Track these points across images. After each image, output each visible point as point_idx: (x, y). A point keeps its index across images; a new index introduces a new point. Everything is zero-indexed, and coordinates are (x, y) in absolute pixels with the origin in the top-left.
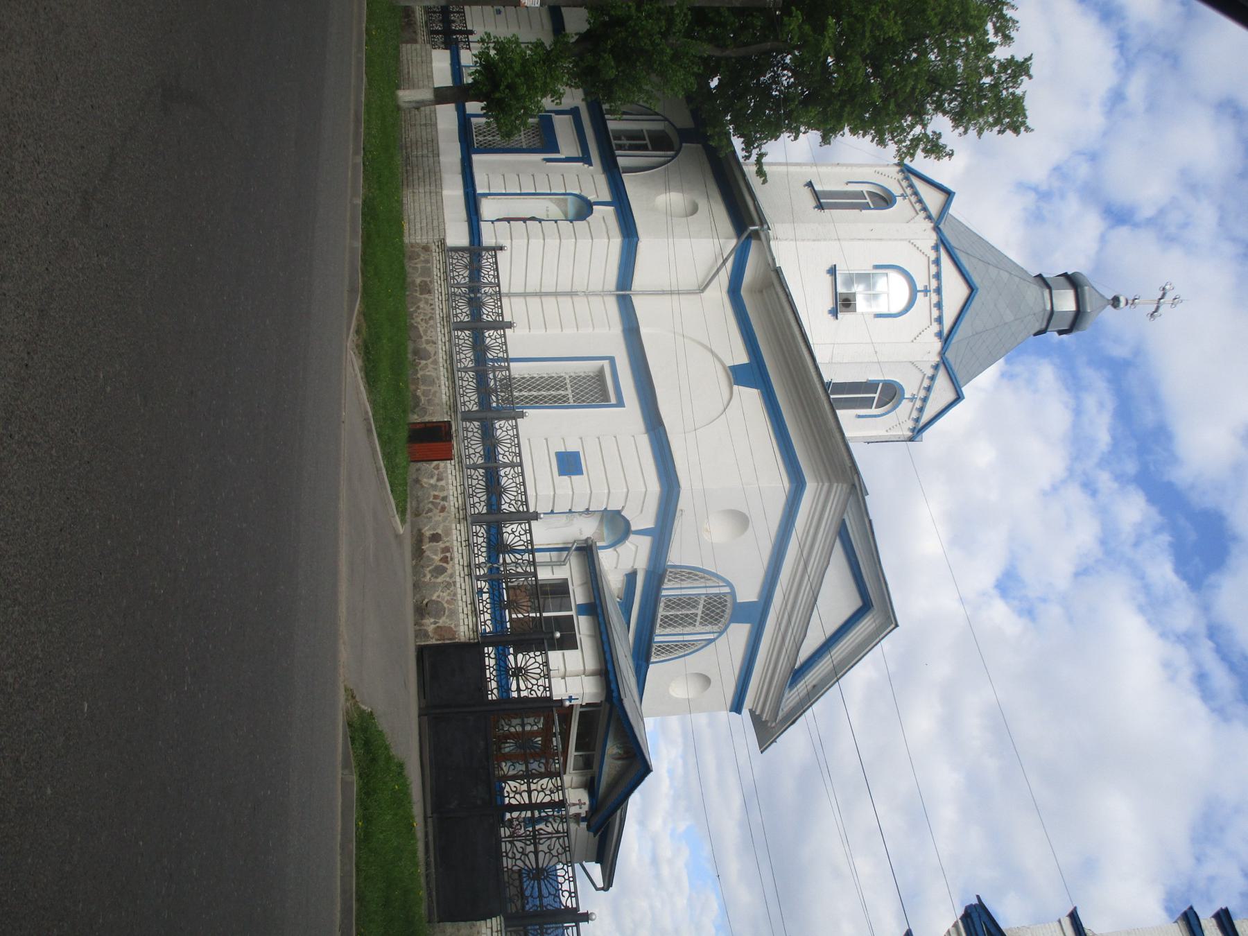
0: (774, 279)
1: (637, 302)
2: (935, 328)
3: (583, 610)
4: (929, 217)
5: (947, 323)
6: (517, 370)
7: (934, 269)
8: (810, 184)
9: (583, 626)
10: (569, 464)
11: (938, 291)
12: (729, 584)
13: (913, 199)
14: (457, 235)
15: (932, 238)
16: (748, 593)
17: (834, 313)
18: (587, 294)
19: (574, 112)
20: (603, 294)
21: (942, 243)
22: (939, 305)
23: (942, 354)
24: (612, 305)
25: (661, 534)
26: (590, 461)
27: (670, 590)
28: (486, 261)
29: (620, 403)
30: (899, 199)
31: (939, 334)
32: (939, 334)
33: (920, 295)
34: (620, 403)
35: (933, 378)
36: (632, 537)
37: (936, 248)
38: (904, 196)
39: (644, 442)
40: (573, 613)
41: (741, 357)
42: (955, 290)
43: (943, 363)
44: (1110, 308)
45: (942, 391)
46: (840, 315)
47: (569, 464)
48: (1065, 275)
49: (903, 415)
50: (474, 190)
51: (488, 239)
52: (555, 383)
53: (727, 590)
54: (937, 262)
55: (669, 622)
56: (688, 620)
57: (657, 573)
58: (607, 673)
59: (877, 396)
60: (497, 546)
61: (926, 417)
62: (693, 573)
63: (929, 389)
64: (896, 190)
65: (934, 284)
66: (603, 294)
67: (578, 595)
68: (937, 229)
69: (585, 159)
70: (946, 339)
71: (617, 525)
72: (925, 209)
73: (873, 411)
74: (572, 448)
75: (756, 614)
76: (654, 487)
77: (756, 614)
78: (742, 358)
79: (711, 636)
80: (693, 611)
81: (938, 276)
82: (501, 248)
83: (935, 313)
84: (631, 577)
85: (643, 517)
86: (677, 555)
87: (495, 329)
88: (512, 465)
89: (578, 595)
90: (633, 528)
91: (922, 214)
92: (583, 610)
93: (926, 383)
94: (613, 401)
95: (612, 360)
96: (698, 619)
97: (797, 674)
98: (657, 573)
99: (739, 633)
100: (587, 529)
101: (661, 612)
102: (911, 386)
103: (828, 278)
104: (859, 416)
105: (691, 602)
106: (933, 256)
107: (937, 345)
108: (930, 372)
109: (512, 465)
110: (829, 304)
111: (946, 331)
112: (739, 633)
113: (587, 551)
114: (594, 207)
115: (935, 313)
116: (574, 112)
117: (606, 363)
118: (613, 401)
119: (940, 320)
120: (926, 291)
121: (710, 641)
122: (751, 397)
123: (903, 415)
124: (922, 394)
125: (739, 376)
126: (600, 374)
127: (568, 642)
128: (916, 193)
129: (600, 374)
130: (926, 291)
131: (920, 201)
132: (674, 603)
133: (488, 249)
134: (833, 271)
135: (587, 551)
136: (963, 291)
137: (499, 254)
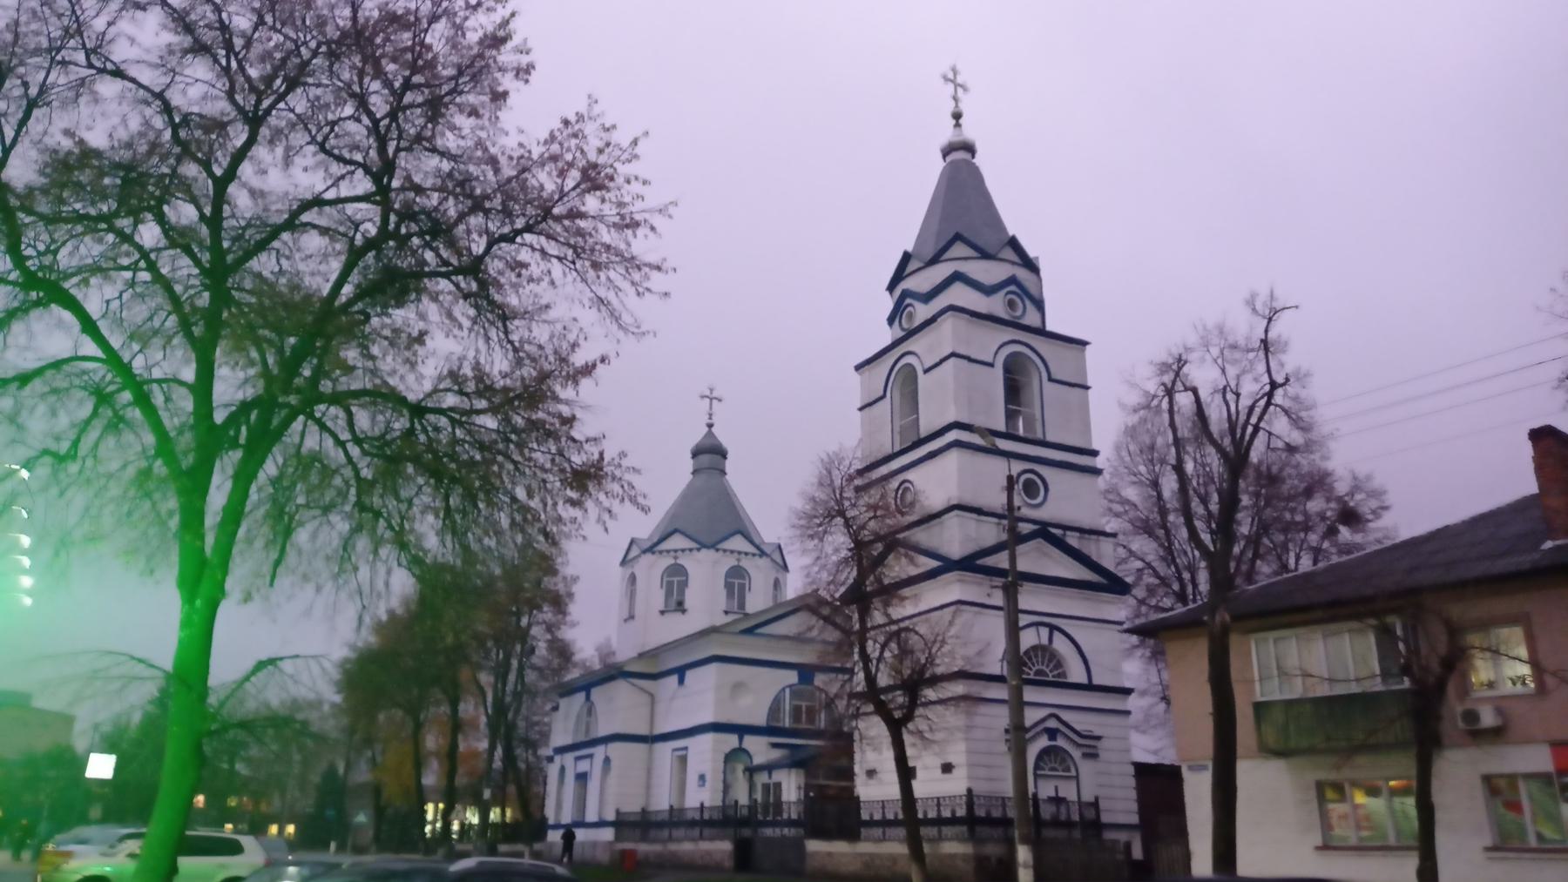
2: (695, 552)
5: (693, 545)
11: (676, 551)
12: (784, 689)
14: (608, 834)
15: (649, 556)
16: (792, 677)
20: (651, 752)
21: (651, 550)
22: (683, 550)
25: (742, 730)
27: (787, 723)
29: (686, 748)
32: (698, 550)
33: (678, 562)
35: (725, 551)
37: (653, 553)
41: (674, 679)
42: (677, 542)
44: (713, 429)
49: (752, 565)
53: (788, 691)
54: (661, 552)
59: (736, 581)
63: (732, 552)
64: (629, 571)
65: (672, 554)
69: (591, 756)
70: (703, 545)
78: (674, 679)
80: (804, 709)
81: (668, 551)
83: (688, 552)
84: (775, 746)
85: (732, 741)
86: (760, 719)
93: (728, 553)
95: (675, 750)
101: (804, 726)
102: (731, 561)
105: (796, 712)
107: (704, 551)
108: (721, 553)
110: (678, 615)
111: (698, 546)
113: (751, 771)
115: (688, 552)
116: (578, 759)
119: (691, 550)
120: (676, 558)
122: (690, 675)
123: (752, 565)
124: (736, 555)
125: (681, 681)
127: (778, 786)
130: (676, 558)
134: (662, 613)
135: (751, 771)
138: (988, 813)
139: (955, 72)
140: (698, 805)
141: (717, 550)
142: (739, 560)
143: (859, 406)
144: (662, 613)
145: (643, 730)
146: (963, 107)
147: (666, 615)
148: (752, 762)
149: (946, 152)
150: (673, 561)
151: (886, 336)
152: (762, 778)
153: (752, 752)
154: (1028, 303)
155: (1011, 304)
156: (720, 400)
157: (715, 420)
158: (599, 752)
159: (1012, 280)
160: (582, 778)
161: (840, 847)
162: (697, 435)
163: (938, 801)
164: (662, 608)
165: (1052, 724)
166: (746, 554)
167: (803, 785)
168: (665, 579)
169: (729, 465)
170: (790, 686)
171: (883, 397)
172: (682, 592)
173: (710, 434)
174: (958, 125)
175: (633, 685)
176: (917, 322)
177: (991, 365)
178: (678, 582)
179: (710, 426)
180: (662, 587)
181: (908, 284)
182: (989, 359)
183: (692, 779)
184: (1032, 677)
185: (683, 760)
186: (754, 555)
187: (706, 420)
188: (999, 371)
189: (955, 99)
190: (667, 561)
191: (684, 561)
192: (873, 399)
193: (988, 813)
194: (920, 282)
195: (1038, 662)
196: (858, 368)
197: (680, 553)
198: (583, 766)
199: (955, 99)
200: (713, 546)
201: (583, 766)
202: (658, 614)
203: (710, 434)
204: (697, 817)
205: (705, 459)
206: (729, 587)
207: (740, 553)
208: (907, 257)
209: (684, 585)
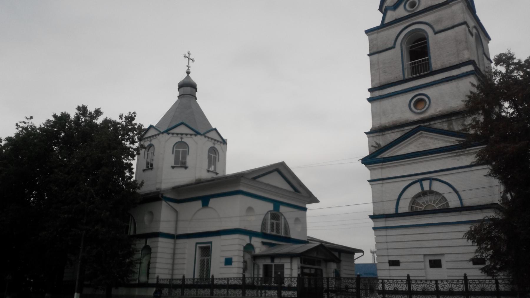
0: (177, 189)
1: (180, 232)
2: (193, 136)
3: (273, 261)
4: (158, 134)
5: (192, 132)
6: (197, 276)
7: (175, 135)
9: (277, 261)
11: (182, 134)
12: (267, 213)
13: (152, 138)
15: (165, 135)
16: (270, 207)
17: (186, 168)
18: (174, 249)
20: (175, 244)
21: (167, 132)
22: (187, 134)
24: (179, 241)
25: (251, 234)
26: (228, 255)
28: (161, 282)
29: (211, 243)
30: (152, 143)
32: (196, 135)
33: (183, 140)
34: (211, 243)
35: (209, 138)
36: (252, 243)
37: (168, 134)
38: (151, 141)
39: (224, 237)
40: (273, 264)
41: (199, 203)
42: (182, 129)
43: (204, 135)
44: (190, 75)
45: (212, 135)
46: (187, 166)
47: (228, 262)
48: (179, 89)
51: (155, 281)
52: (202, 263)
53: (269, 213)
54: (173, 134)
55: (278, 230)
56: (278, 225)
57: (263, 235)
58: (291, 256)
60: (252, 287)
61: (220, 139)
62: (264, 224)
63: (212, 139)
66: (175, 244)
67: (268, 262)
68: (163, 133)
70: (197, 133)
71: (249, 248)
72: (155, 135)
73: (217, 156)
74: (223, 260)
75: (277, 204)
76: (236, 236)
77: (277, 204)
78: (199, 203)
79: (283, 218)
81: (177, 134)
82: (158, 277)
83: (189, 136)
84: (264, 243)
85: (246, 239)
87: (185, 281)
88: (228, 281)
89: (268, 262)
91: (157, 136)
92: (273, 261)
93: (210, 140)
94: (210, 245)
95: (197, 244)
96: (278, 222)
97: (296, 190)
98: (263, 235)
99: (283, 209)
100: (248, 257)
101: (274, 233)
102: (210, 144)
104: (218, 161)
105: (272, 224)
106: (170, 135)
107: (199, 136)
108: (207, 139)
109: (228, 281)
110: (183, 169)
112: (283, 209)
113: (255, 258)
114: (147, 244)
117: (198, 245)
118: (210, 245)
119: (191, 135)
120: (182, 138)
121: (285, 218)
122: (212, 202)
124: (213, 141)
126: (201, 248)
127: (282, 267)
128: (150, 137)
129: (201, 248)
130: (182, 138)
131: (153, 136)
132: (272, 230)
134: (173, 167)
137: (160, 278)
141: (205, 137)
143: (369, 53)
144: (173, 167)
145: (171, 231)
147: (175, 169)
150: (179, 140)
152: (262, 263)
156: (193, 61)
157: (191, 70)
164: (173, 165)
167: (300, 267)
168: (175, 149)
169: (197, 94)
170: (270, 211)
171: (393, 47)
172: (184, 158)
173: (188, 77)
175: (169, 205)
176: (421, 8)
178: (182, 151)
179: (188, 73)
180: (173, 153)
185: (206, 251)
190: (177, 139)
191: (186, 140)
192: (380, 50)
196: (367, 32)
197: (184, 136)
202: (171, 169)
203: (188, 77)
205: (188, 90)
209: (185, 154)
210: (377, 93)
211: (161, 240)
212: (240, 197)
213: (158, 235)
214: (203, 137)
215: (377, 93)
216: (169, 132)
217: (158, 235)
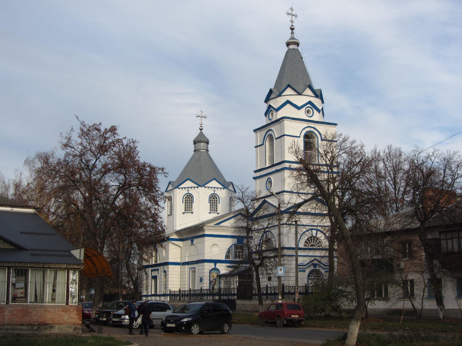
2: (196, 188)
5: (196, 186)
8: (169, 215)
10: (201, 280)
12: (232, 246)
19: (152, 271)
23: (201, 187)
25: (216, 262)
28: (172, 293)
29: (195, 268)
31: (197, 187)
34: (195, 268)
35: (208, 187)
42: (188, 184)
44: (202, 131)
50: (162, 294)
53: (233, 246)
54: (182, 188)
63: (211, 188)
65: (187, 189)
69: (158, 270)
70: (199, 186)
81: (185, 188)
82: (170, 290)
84: (228, 267)
85: (212, 265)
86: (223, 258)
90: (214, 267)
95: (190, 268)
102: (211, 192)
103: (185, 214)
104: (219, 203)
107: (200, 188)
110: (191, 213)
116: (152, 271)
119: (194, 187)
120: (188, 191)
133: (170, 293)
134: (184, 213)
136: (188, 181)
138: (289, 291)
139: (292, 9)
140: (200, 288)
142: (214, 191)
143: (255, 146)
146: (295, 25)
148: (220, 273)
149: (288, 44)
151: (264, 121)
153: (220, 269)
154: (315, 111)
155: (308, 112)
158: (161, 269)
159: (310, 103)
160: (155, 278)
161: (247, 302)
162: (195, 134)
163: (275, 288)
165: (315, 262)
166: (218, 188)
170: (234, 245)
174: (292, 33)
177: (299, 137)
180: (183, 203)
181: (272, 103)
182: (299, 136)
183: (197, 280)
184: (309, 247)
186: (221, 188)
187: (199, 127)
188: (302, 138)
189: (292, 22)
191: (191, 191)
193: (289, 291)
194: (275, 103)
195: (312, 242)
196: (255, 131)
197: (190, 189)
198: (154, 274)
199: (292, 22)
200: (204, 186)
201: (154, 274)
204: (200, 292)
206: (210, 201)
207: (215, 188)
208: (271, 91)
210: (258, 174)
211: (170, 266)
212: (206, 238)
213: (167, 264)
214: (203, 188)
215: (258, 174)
216: (179, 187)
217: (167, 264)
